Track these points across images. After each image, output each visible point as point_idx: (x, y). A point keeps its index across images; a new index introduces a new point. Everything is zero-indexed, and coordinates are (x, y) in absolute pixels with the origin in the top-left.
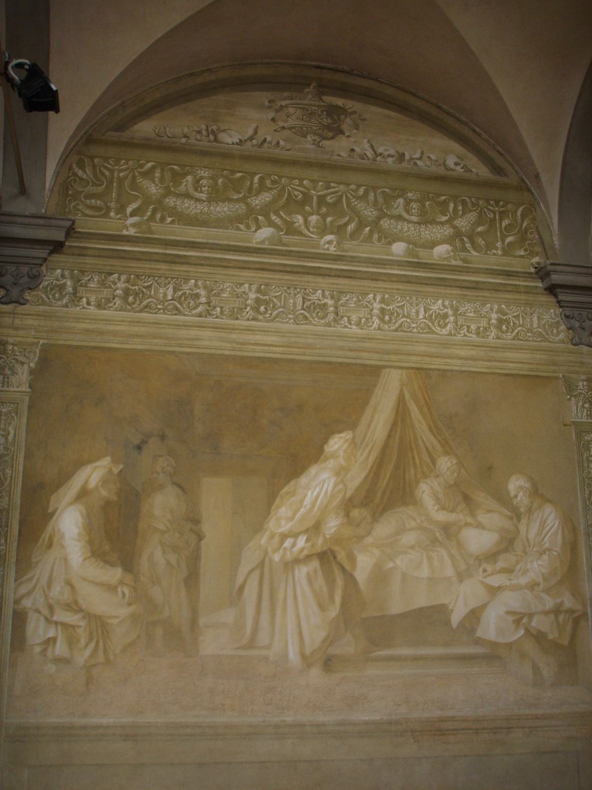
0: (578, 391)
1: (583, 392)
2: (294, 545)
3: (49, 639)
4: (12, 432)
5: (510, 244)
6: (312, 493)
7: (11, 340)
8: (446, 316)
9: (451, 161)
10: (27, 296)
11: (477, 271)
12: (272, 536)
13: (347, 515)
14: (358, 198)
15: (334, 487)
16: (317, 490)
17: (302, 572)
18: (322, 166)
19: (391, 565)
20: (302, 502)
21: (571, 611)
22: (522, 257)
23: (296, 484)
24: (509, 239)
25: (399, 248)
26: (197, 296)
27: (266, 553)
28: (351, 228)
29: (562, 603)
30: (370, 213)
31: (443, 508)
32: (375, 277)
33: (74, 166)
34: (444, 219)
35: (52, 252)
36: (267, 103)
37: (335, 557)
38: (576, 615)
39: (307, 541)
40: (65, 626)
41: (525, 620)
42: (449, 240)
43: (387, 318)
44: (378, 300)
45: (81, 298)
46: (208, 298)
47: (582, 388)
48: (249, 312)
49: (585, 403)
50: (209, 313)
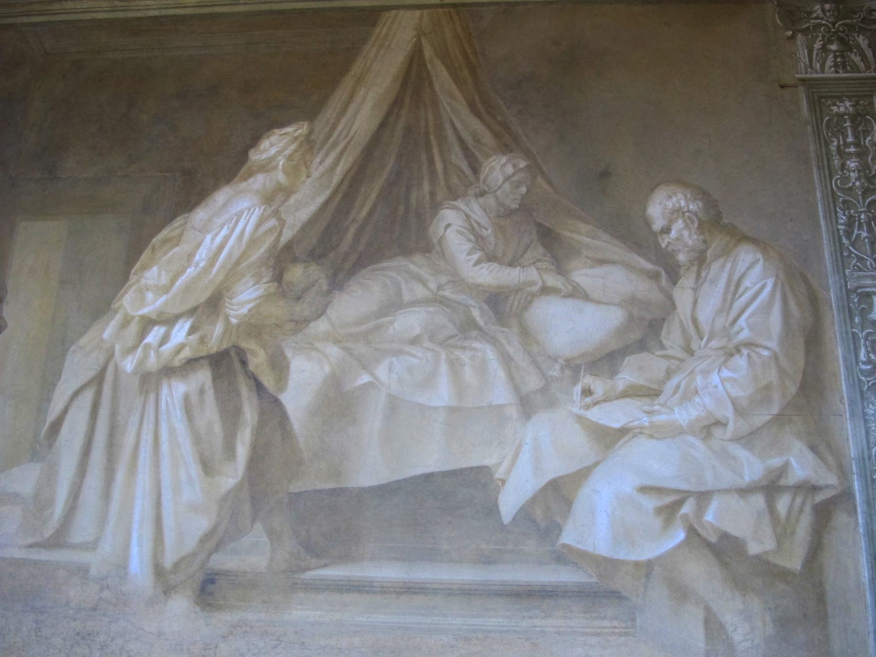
0: (812, 21)
1: (824, 22)
2: (165, 340)
6: (213, 239)
12: (126, 322)
13: (278, 278)
15: (258, 225)
16: (224, 232)
19: (365, 378)
20: (191, 256)
21: (808, 488)
23: (185, 223)
27: (111, 356)
29: (783, 470)
31: (491, 258)
37: (244, 363)
38: (820, 498)
39: (192, 330)
41: (687, 508)
47: (821, 15)
49: (830, 42)
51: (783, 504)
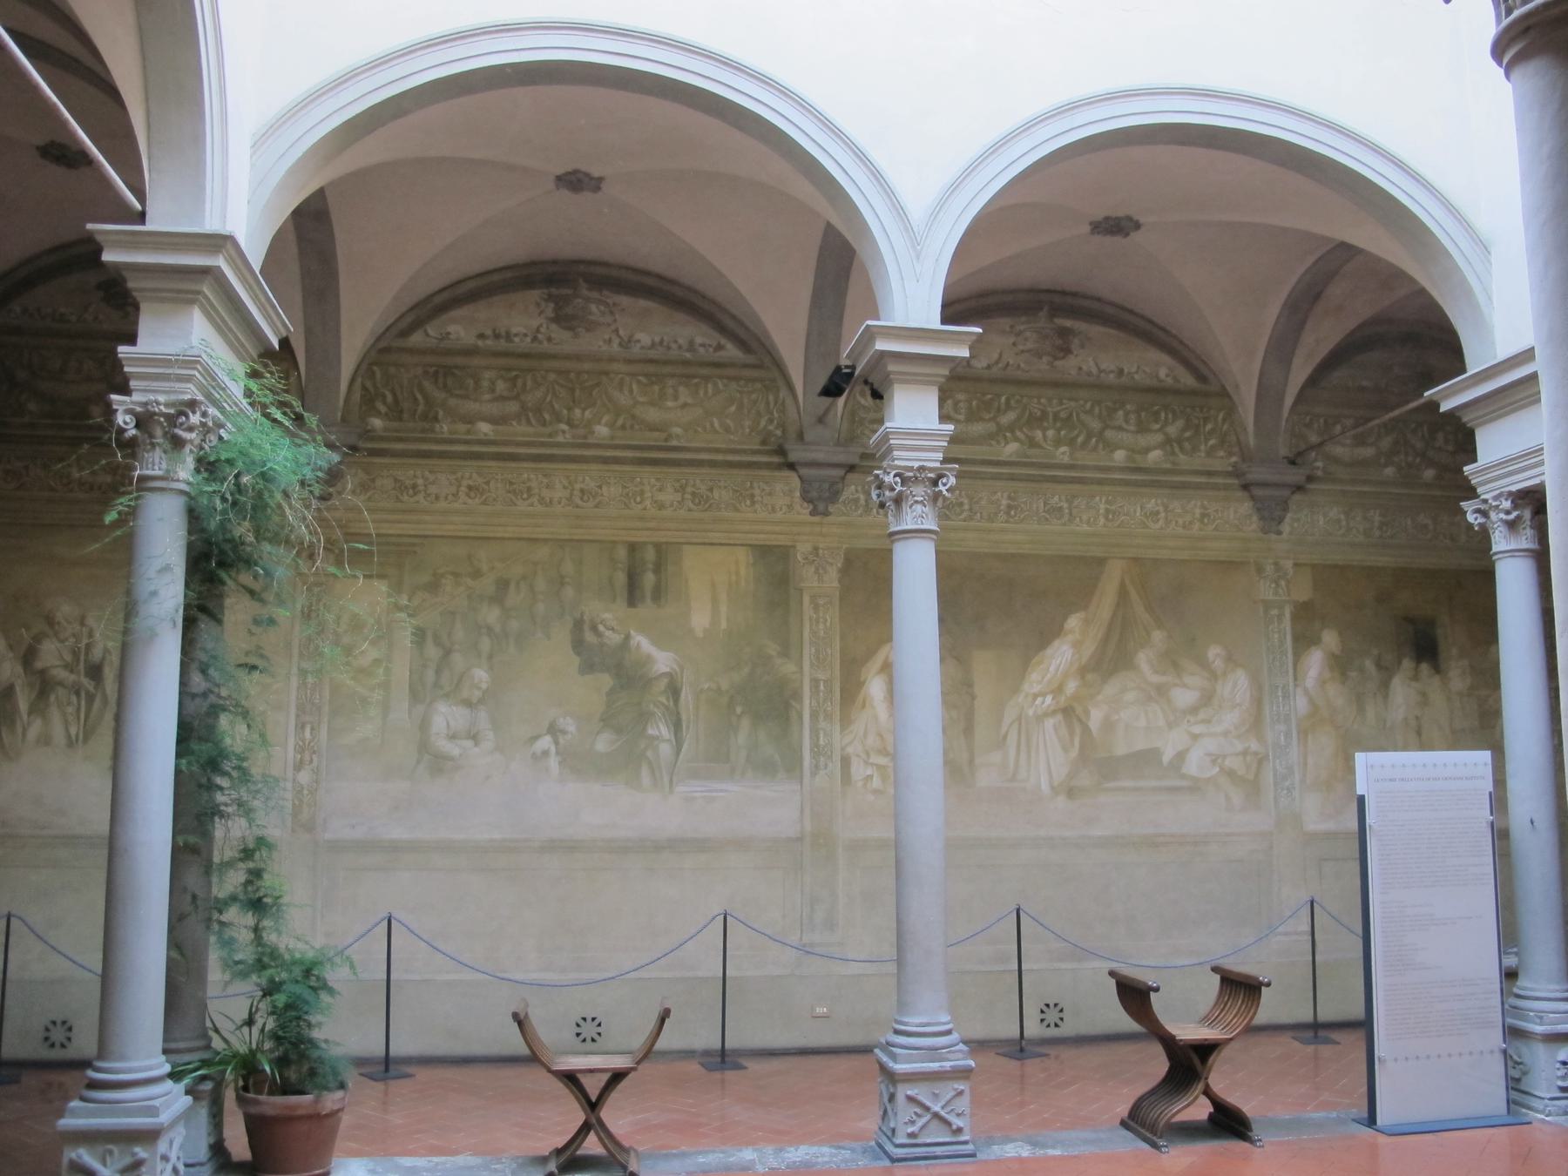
2: (1043, 703)
3: (868, 776)
4: (829, 620)
5: (1212, 447)
7: (821, 546)
8: (1158, 513)
9: (1163, 373)
10: (831, 509)
11: (1182, 472)
13: (1083, 677)
14: (1086, 412)
15: (1073, 655)
16: (1060, 659)
17: (1049, 723)
18: (1055, 385)
19: (1116, 717)
21: (1256, 754)
22: (1222, 458)
24: (1212, 442)
25: (1120, 455)
26: (961, 504)
28: (1080, 440)
30: (1096, 425)
31: (1156, 672)
32: (1100, 482)
33: (858, 395)
34: (1157, 426)
35: (848, 472)
36: (1008, 329)
37: (1074, 712)
38: (1260, 756)
39: (1053, 699)
40: (880, 767)
41: (1219, 761)
42: (1161, 446)
43: (1111, 516)
44: (1103, 501)
45: (872, 509)
46: (970, 505)
48: (1002, 516)
50: (970, 518)
51: (1248, 758)
